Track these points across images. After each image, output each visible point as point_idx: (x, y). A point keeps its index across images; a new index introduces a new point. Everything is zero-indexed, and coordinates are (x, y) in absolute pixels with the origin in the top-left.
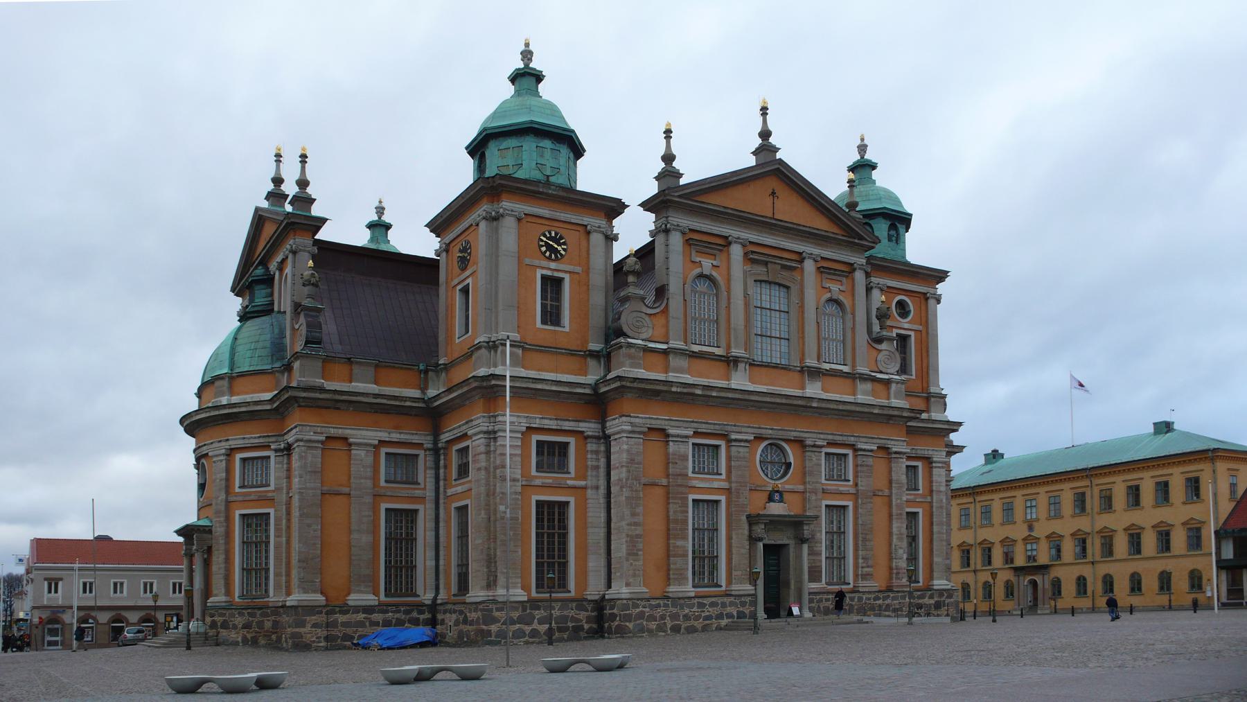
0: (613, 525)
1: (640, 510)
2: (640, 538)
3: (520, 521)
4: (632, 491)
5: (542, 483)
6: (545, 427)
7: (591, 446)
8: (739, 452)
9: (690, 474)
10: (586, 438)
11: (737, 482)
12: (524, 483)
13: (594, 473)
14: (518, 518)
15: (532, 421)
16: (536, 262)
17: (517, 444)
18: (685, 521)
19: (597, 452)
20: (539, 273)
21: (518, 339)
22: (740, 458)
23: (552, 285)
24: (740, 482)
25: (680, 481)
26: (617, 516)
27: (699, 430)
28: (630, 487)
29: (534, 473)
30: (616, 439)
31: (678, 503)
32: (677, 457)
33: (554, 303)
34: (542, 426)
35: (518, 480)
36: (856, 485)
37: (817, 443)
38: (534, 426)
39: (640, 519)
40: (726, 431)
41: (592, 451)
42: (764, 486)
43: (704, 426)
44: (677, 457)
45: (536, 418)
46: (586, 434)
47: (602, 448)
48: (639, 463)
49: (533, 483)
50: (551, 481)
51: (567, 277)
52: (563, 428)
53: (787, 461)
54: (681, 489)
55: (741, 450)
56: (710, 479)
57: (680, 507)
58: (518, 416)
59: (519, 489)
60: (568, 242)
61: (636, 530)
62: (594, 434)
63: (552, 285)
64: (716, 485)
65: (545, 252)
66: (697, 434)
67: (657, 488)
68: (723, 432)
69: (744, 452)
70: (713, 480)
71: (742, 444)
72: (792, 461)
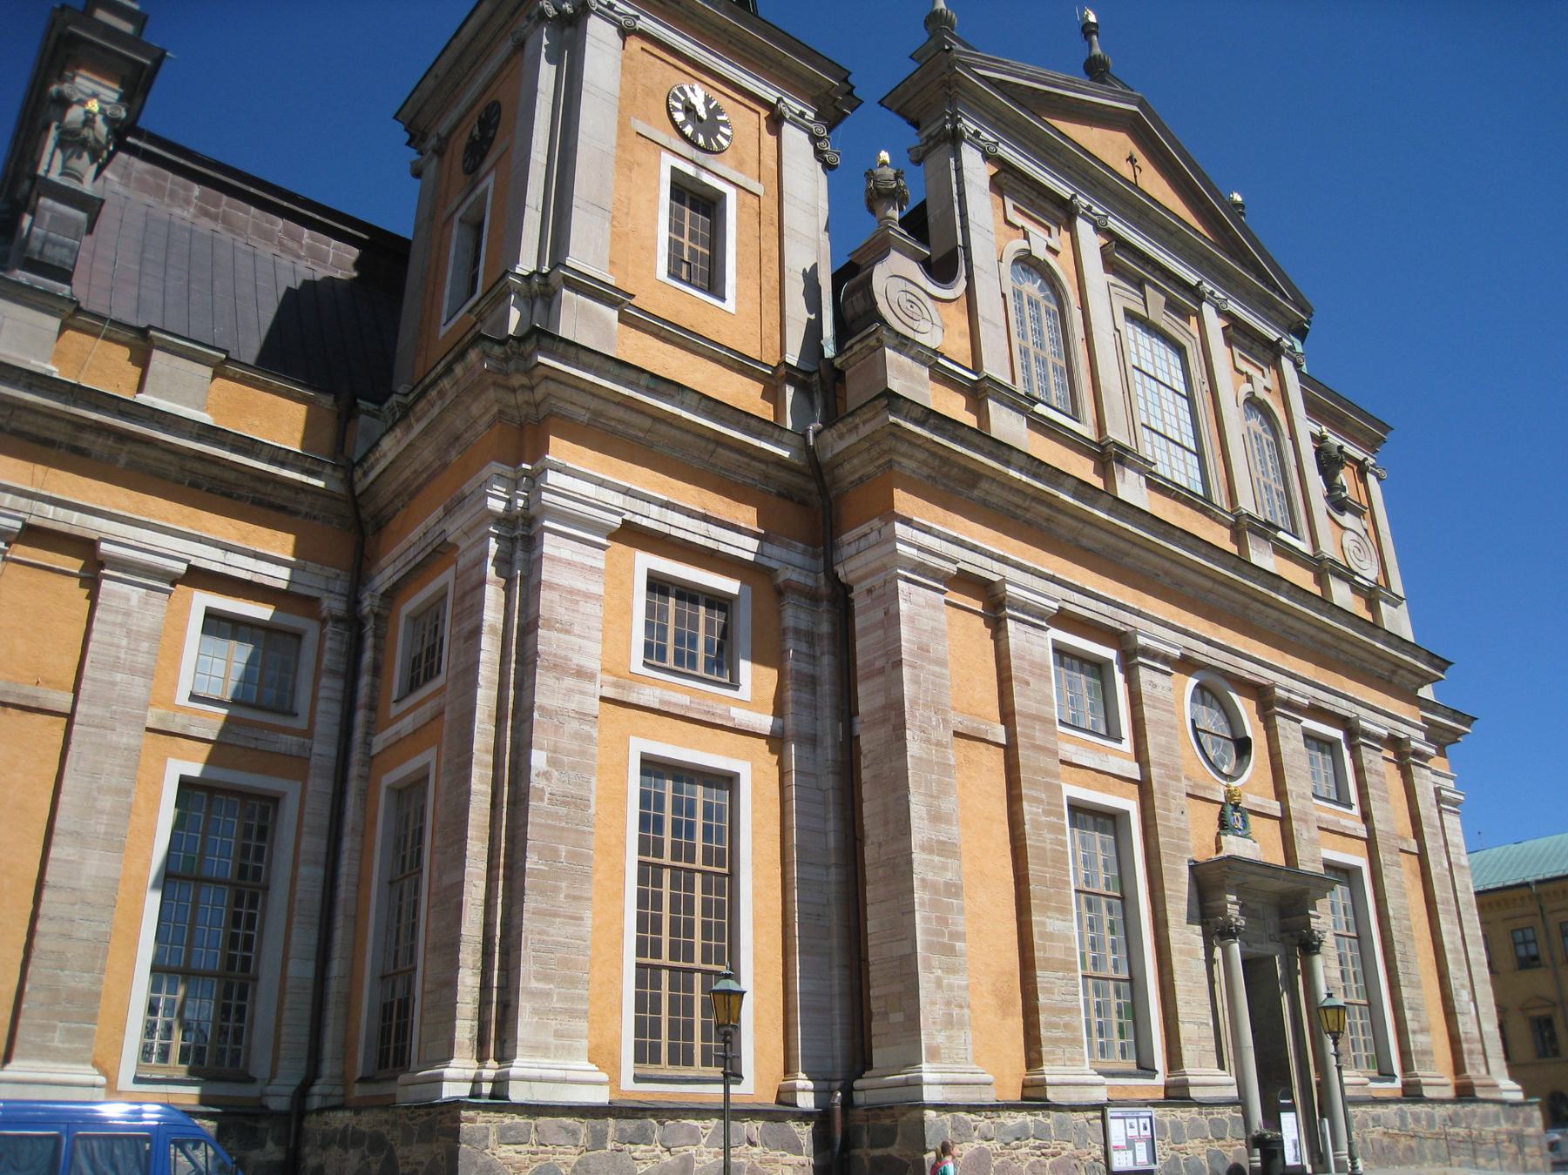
0: (870, 853)
2: (957, 895)
3: (592, 811)
4: (928, 741)
5: (662, 702)
7: (794, 616)
8: (1155, 686)
10: (780, 592)
12: (610, 692)
13: (805, 697)
15: (639, 505)
16: (662, 138)
17: (590, 562)
18: (1060, 860)
19: (810, 637)
26: (886, 823)
30: (870, 591)
32: (1026, 665)
33: (699, 249)
34: (666, 529)
36: (1366, 817)
37: (1294, 697)
39: (954, 832)
41: (797, 631)
46: (781, 579)
47: (825, 628)
48: (942, 663)
49: (633, 699)
50: (685, 699)
52: (723, 548)
53: (1240, 736)
55: (1158, 678)
57: (1047, 813)
59: (594, 706)
60: (733, 122)
61: (944, 868)
62: (802, 580)
65: (684, 124)
66: (1064, 619)
67: (981, 745)
68: (1117, 625)
72: (1249, 734)
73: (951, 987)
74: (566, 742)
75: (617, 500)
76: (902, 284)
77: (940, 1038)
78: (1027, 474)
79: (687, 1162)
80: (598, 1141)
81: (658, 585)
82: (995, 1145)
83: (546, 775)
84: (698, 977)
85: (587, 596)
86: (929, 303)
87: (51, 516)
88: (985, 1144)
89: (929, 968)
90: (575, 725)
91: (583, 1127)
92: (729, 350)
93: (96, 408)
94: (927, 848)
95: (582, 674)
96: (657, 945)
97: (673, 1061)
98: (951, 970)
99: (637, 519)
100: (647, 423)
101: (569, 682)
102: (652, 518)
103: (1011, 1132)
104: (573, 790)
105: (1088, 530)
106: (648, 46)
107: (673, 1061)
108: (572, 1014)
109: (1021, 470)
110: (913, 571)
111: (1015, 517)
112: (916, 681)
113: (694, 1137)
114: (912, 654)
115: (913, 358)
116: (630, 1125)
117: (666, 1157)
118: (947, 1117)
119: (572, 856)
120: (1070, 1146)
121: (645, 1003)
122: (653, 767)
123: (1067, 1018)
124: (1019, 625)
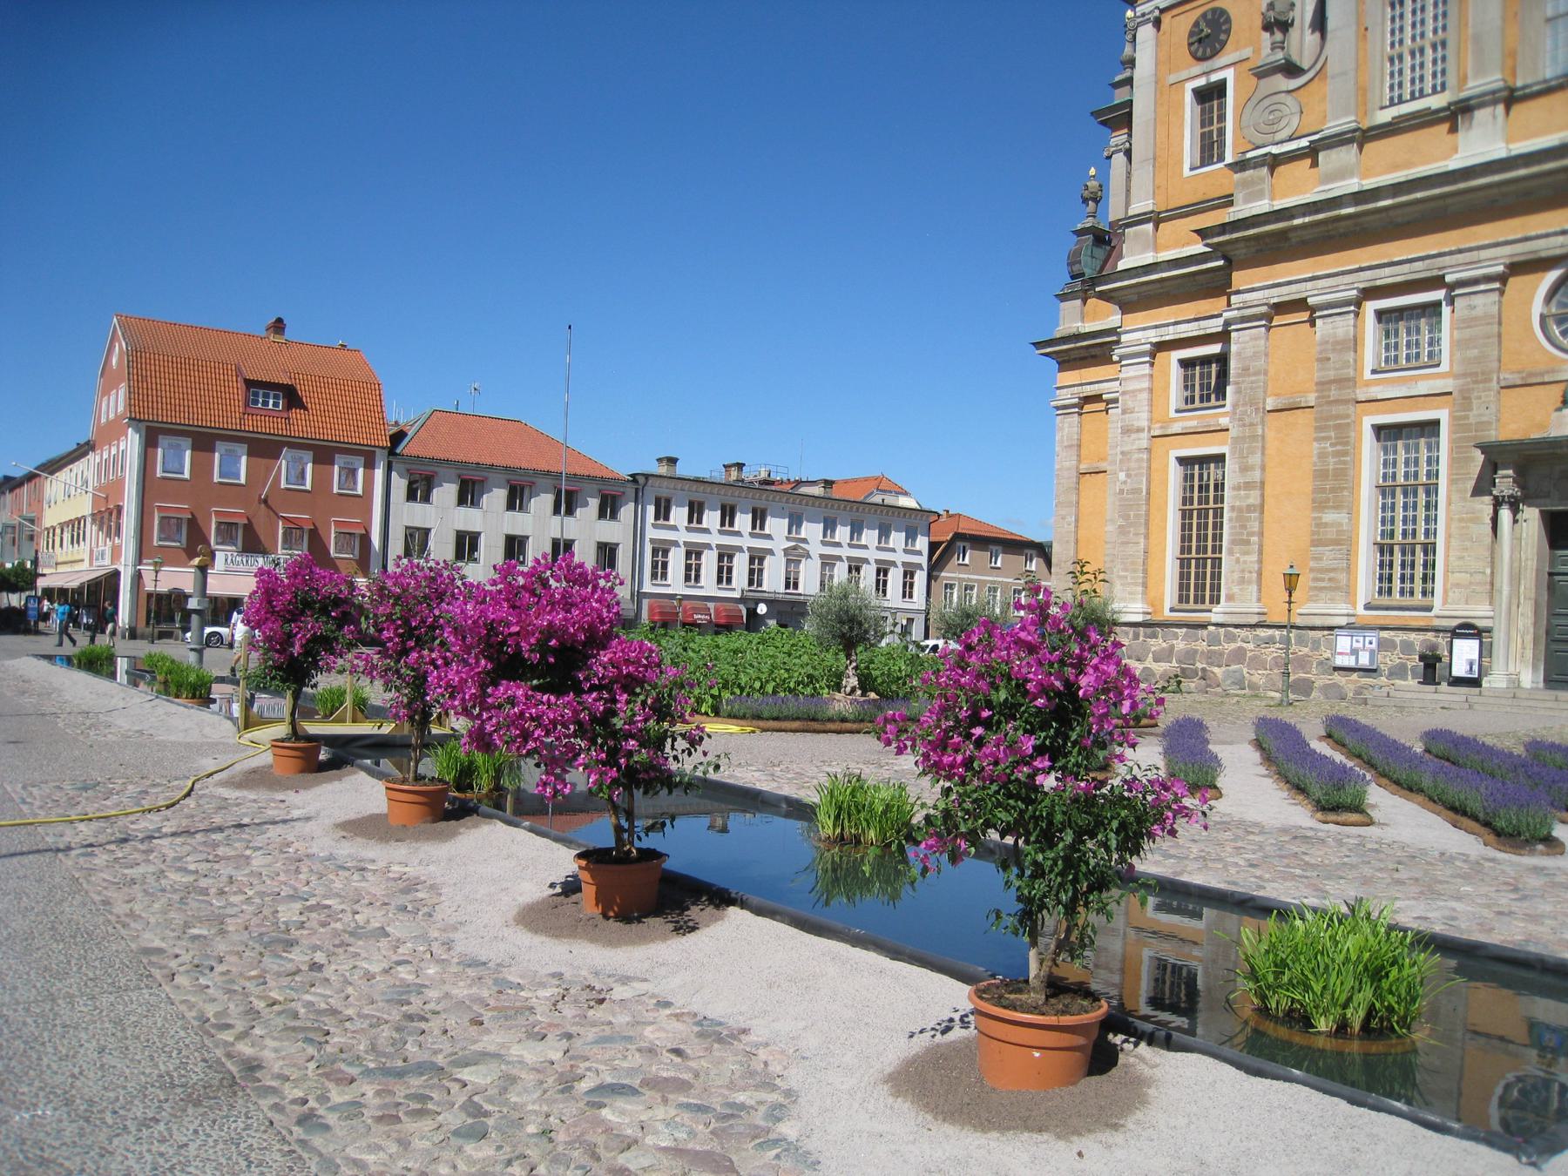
1: (1256, 459)
4: (1244, 425)
6: (1182, 336)
9: (1367, 375)
11: (1465, 375)
14: (1141, 489)
16: (1184, 75)
20: (1190, 86)
21: (1151, 208)
22: (1475, 319)
23: (1211, 95)
24: (1476, 374)
25: (1334, 393)
27: (1378, 283)
28: (1240, 420)
29: (1172, 414)
31: (1328, 438)
34: (1177, 336)
35: (1139, 430)
38: (1167, 338)
40: (1440, 269)
42: (1553, 371)
43: (1387, 271)
44: (1330, 347)
45: (1168, 325)
50: (1194, 423)
51: (1229, 74)
52: (1209, 331)
54: (1341, 409)
55: (1478, 300)
56: (1411, 378)
58: (1144, 329)
61: (1247, 497)
63: (1211, 95)
64: (1423, 388)
68: (1435, 273)
69: (1485, 305)
70: (1415, 379)
71: (1482, 287)
73: (1245, 562)
74: (1133, 465)
75: (1152, 333)
76: (1267, 102)
77: (1236, 589)
78: (1310, 214)
79: (1172, 647)
80: (1136, 637)
81: (1186, 364)
82: (1251, 646)
83: (1125, 482)
84: (1209, 561)
85: (1140, 391)
86: (1289, 99)
87: (1089, 390)
88: (1245, 645)
89: (1231, 552)
90: (1136, 456)
91: (1131, 630)
92: (1219, 198)
93: (1085, 340)
94: (1237, 488)
95: (1139, 430)
96: (1190, 548)
97: (1196, 602)
98: (1247, 553)
99: (1164, 339)
100: (1158, 285)
101: (1134, 436)
102: (1170, 334)
103: (1261, 639)
104: (1136, 486)
105: (1391, 213)
106: (1175, 12)
107: (1196, 602)
108: (1135, 584)
109: (1304, 215)
110: (1242, 323)
111: (1331, 237)
112: (1238, 391)
113: (1176, 636)
114: (1239, 375)
115: (1255, 168)
116: (1149, 630)
117: (1164, 645)
118: (1222, 630)
119: (1136, 516)
120: (1306, 650)
121: (1184, 576)
122: (1182, 461)
123: (1332, 575)
124: (1330, 320)
